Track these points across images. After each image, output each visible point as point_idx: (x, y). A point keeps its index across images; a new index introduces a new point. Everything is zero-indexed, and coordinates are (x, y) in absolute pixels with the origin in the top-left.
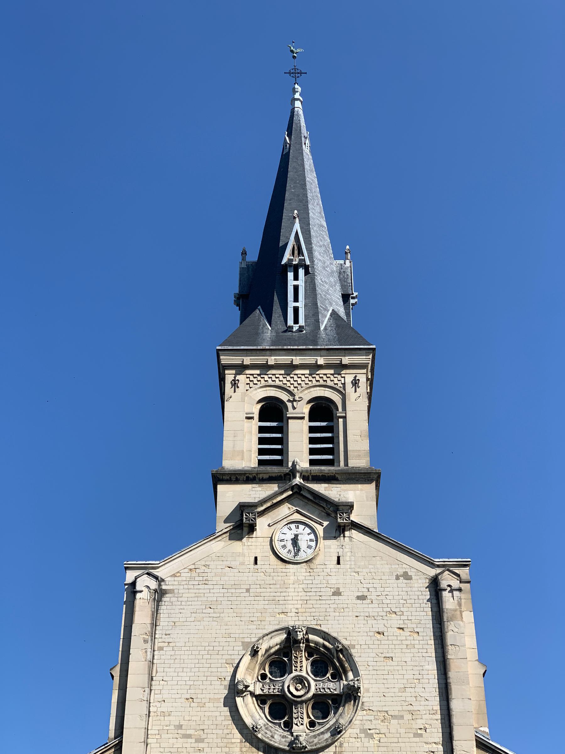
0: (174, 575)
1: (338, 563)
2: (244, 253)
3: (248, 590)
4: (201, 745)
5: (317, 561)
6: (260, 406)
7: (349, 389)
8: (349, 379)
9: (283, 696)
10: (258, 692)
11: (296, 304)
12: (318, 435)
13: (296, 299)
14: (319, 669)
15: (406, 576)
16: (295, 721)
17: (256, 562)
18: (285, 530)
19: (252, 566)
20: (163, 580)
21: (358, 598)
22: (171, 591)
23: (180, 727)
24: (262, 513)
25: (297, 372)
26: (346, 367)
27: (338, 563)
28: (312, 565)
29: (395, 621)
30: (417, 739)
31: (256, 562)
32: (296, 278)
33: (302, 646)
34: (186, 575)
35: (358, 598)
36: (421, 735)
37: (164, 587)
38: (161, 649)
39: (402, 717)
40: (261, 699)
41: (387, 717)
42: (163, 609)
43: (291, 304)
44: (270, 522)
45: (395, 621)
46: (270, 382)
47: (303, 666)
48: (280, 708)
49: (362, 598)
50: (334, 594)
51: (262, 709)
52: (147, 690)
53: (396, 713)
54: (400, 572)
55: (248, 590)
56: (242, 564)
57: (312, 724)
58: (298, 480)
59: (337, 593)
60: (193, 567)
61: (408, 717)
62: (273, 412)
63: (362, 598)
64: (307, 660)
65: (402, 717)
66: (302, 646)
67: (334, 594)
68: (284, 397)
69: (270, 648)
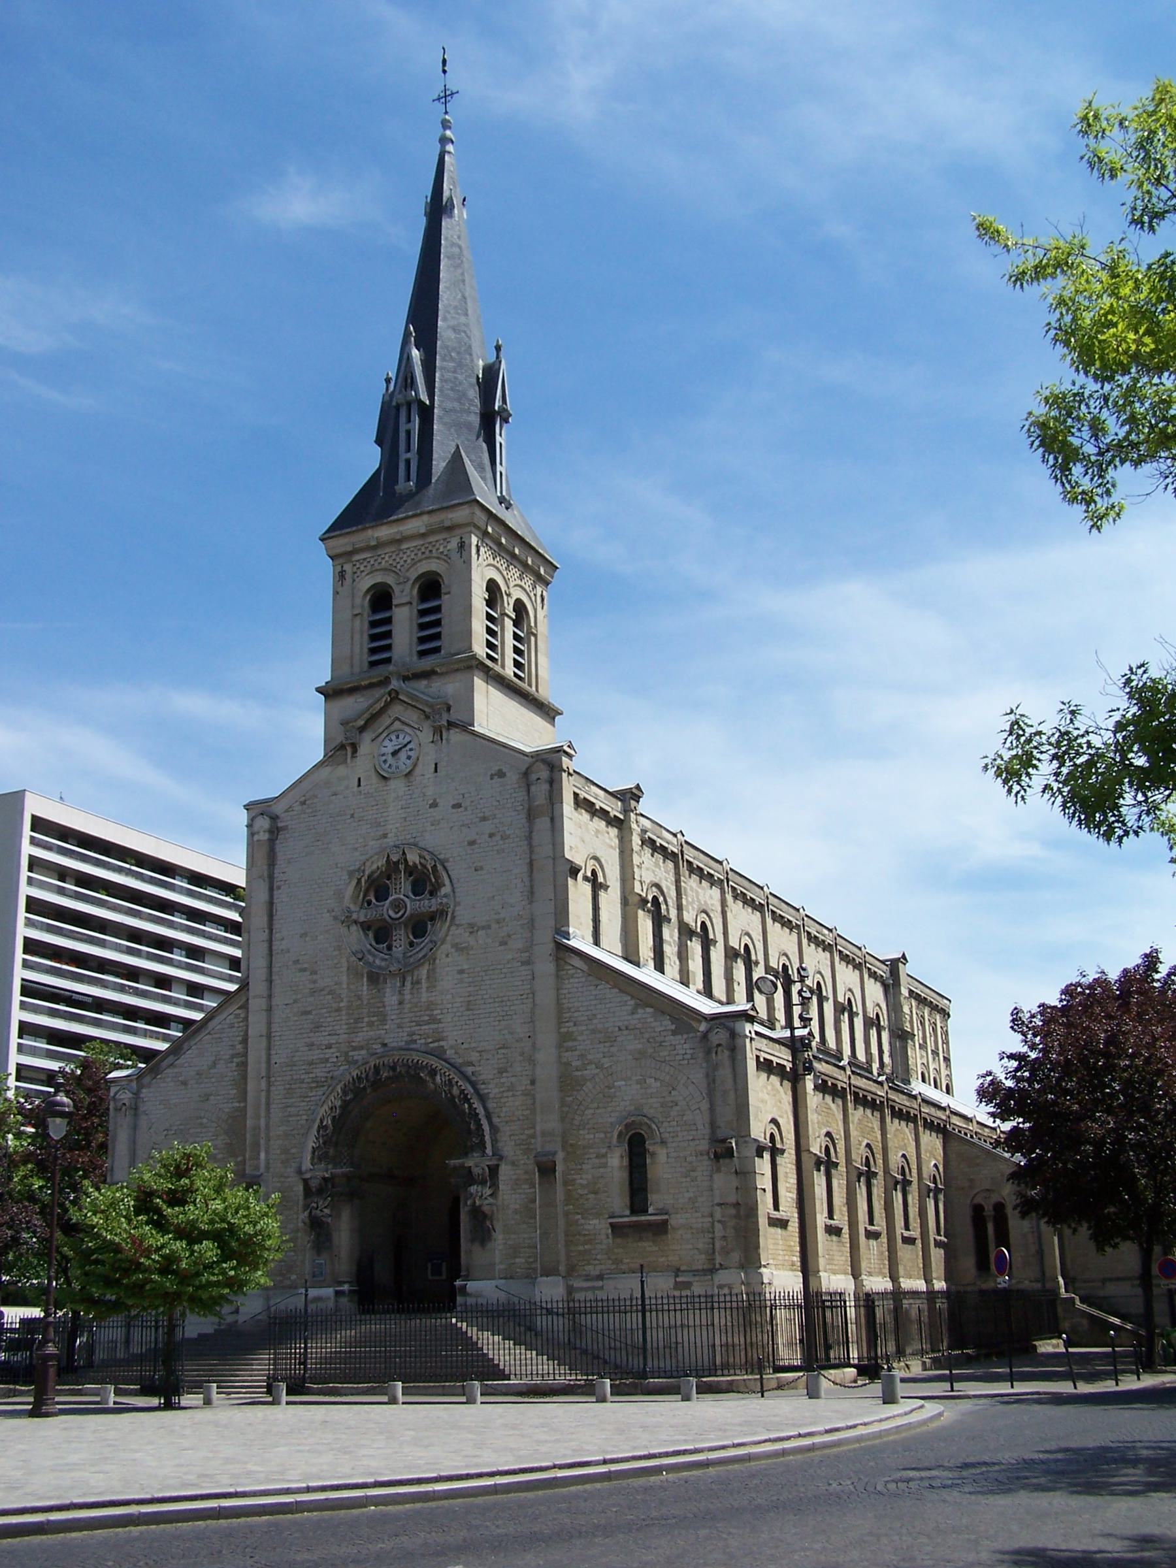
0: (286, 811)
1: (436, 771)
2: (388, 381)
3: (352, 816)
4: (315, 977)
5: (418, 771)
6: (368, 598)
7: (455, 556)
8: (454, 544)
9: (385, 920)
10: (362, 919)
11: (409, 455)
12: (427, 619)
13: (408, 450)
14: (419, 887)
15: (501, 774)
16: (394, 944)
17: (359, 785)
18: (387, 743)
19: (356, 788)
20: (277, 817)
21: (454, 806)
22: (285, 828)
23: (297, 962)
24: (362, 729)
25: (404, 546)
26: (449, 529)
27: (436, 771)
28: (412, 779)
29: (488, 827)
30: (502, 948)
31: (359, 785)
32: (409, 421)
33: (402, 867)
34: (297, 808)
35: (454, 806)
36: (506, 943)
37: (280, 825)
38: (279, 888)
39: (489, 927)
40: (366, 927)
41: (473, 929)
42: (278, 848)
43: (403, 456)
44: (374, 736)
45: (488, 827)
46: (377, 567)
47: (402, 888)
48: (381, 933)
49: (457, 806)
50: (431, 806)
51: (367, 935)
52: (267, 931)
53: (484, 924)
54: (495, 769)
55: (352, 816)
56: (347, 788)
57: (411, 944)
58: (395, 684)
59: (434, 805)
60: (303, 799)
61: (494, 926)
62: (381, 599)
63: (457, 806)
64: (406, 879)
65: (489, 927)
66: (402, 867)
67: (431, 806)
68: (390, 580)
69: (373, 873)
